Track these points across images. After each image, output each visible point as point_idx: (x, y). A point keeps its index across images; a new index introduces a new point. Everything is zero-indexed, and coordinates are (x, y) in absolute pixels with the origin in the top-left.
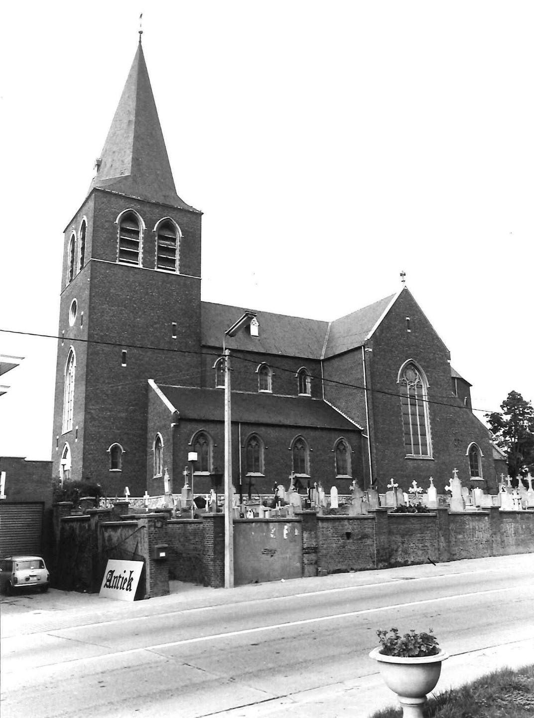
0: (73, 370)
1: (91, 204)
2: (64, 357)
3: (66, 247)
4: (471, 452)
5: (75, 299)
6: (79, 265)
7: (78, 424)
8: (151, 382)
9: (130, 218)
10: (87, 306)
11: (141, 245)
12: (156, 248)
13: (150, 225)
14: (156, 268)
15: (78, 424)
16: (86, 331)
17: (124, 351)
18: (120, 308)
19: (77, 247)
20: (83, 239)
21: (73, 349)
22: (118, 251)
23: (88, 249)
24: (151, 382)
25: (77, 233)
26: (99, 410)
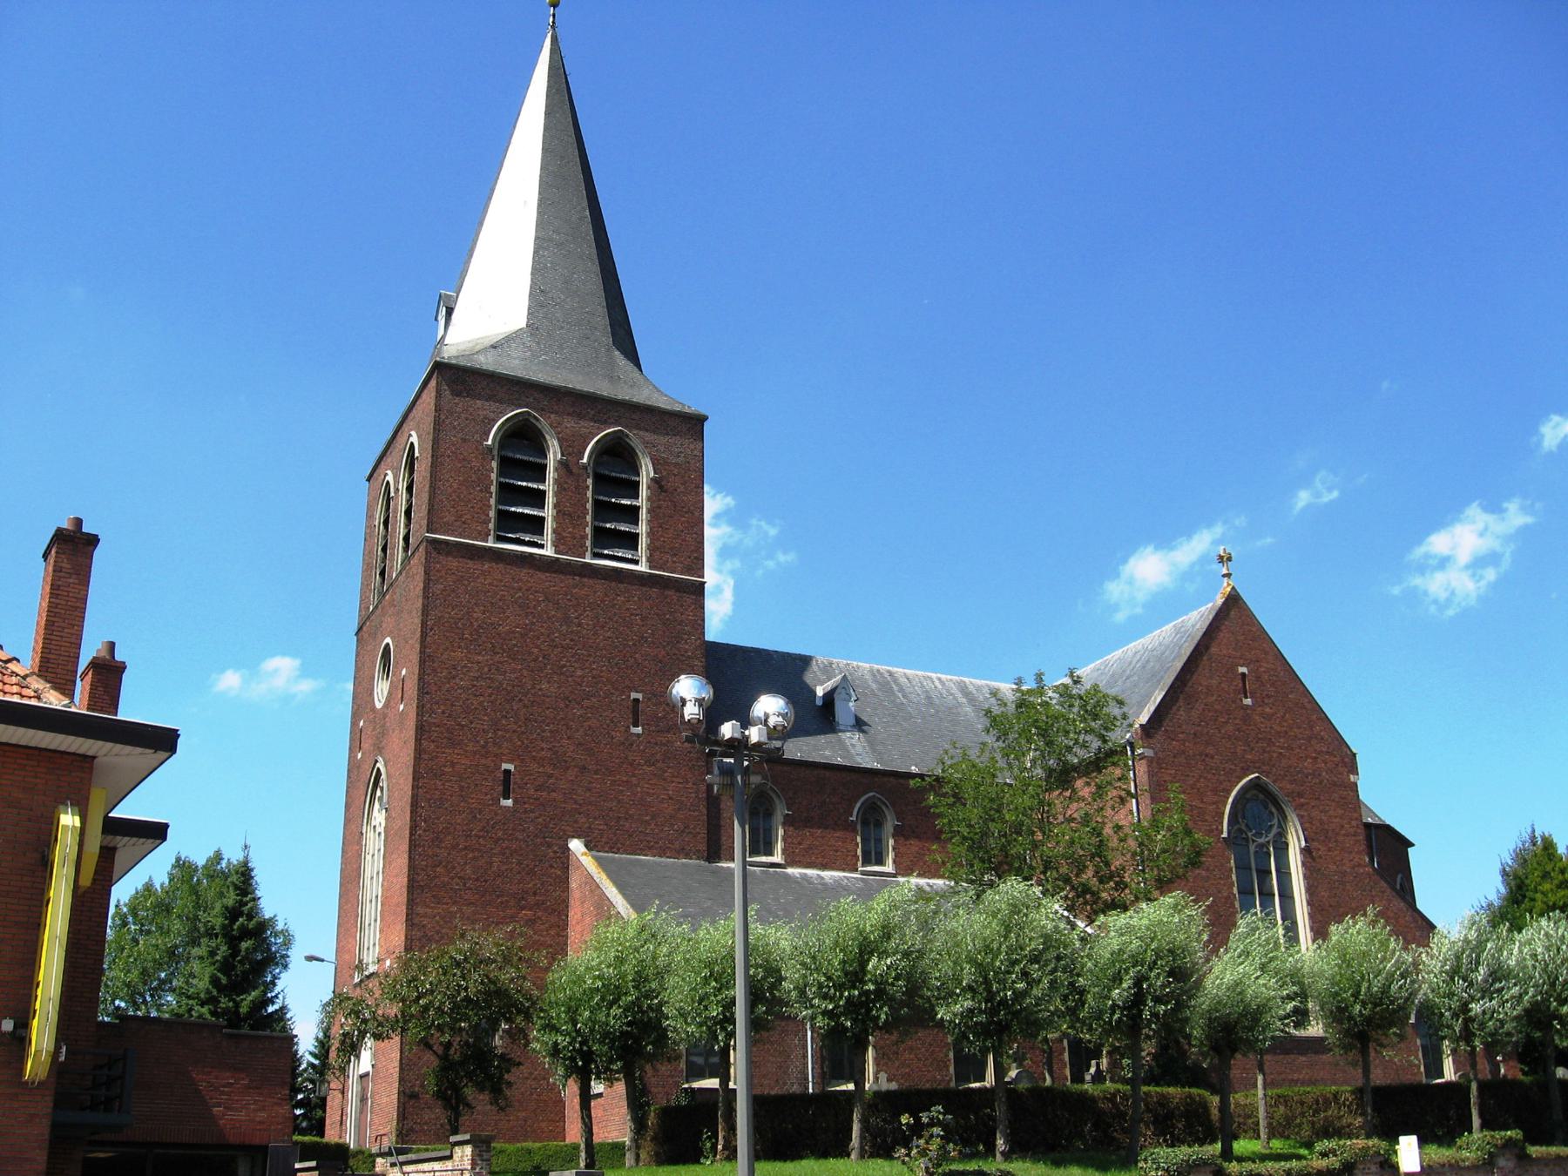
0: (379, 817)
1: (429, 397)
2: (362, 786)
3: (370, 517)
4: (20, 1032)
5: (388, 640)
6: (400, 555)
7: (390, 953)
8: (576, 845)
9: (523, 436)
10: (415, 658)
11: (550, 500)
12: (589, 506)
13: (571, 448)
14: (588, 554)
15: (390, 953)
16: (413, 715)
17: (505, 766)
18: (497, 658)
19: (395, 511)
20: (410, 489)
21: (380, 765)
22: (492, 514)
23: (420, 514)
24: (576, 845)
25: (396, 477)
26: (442, 918)
